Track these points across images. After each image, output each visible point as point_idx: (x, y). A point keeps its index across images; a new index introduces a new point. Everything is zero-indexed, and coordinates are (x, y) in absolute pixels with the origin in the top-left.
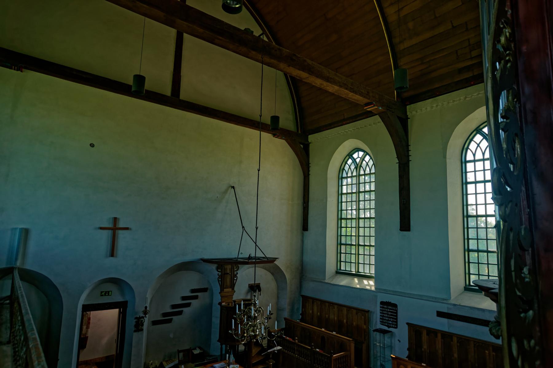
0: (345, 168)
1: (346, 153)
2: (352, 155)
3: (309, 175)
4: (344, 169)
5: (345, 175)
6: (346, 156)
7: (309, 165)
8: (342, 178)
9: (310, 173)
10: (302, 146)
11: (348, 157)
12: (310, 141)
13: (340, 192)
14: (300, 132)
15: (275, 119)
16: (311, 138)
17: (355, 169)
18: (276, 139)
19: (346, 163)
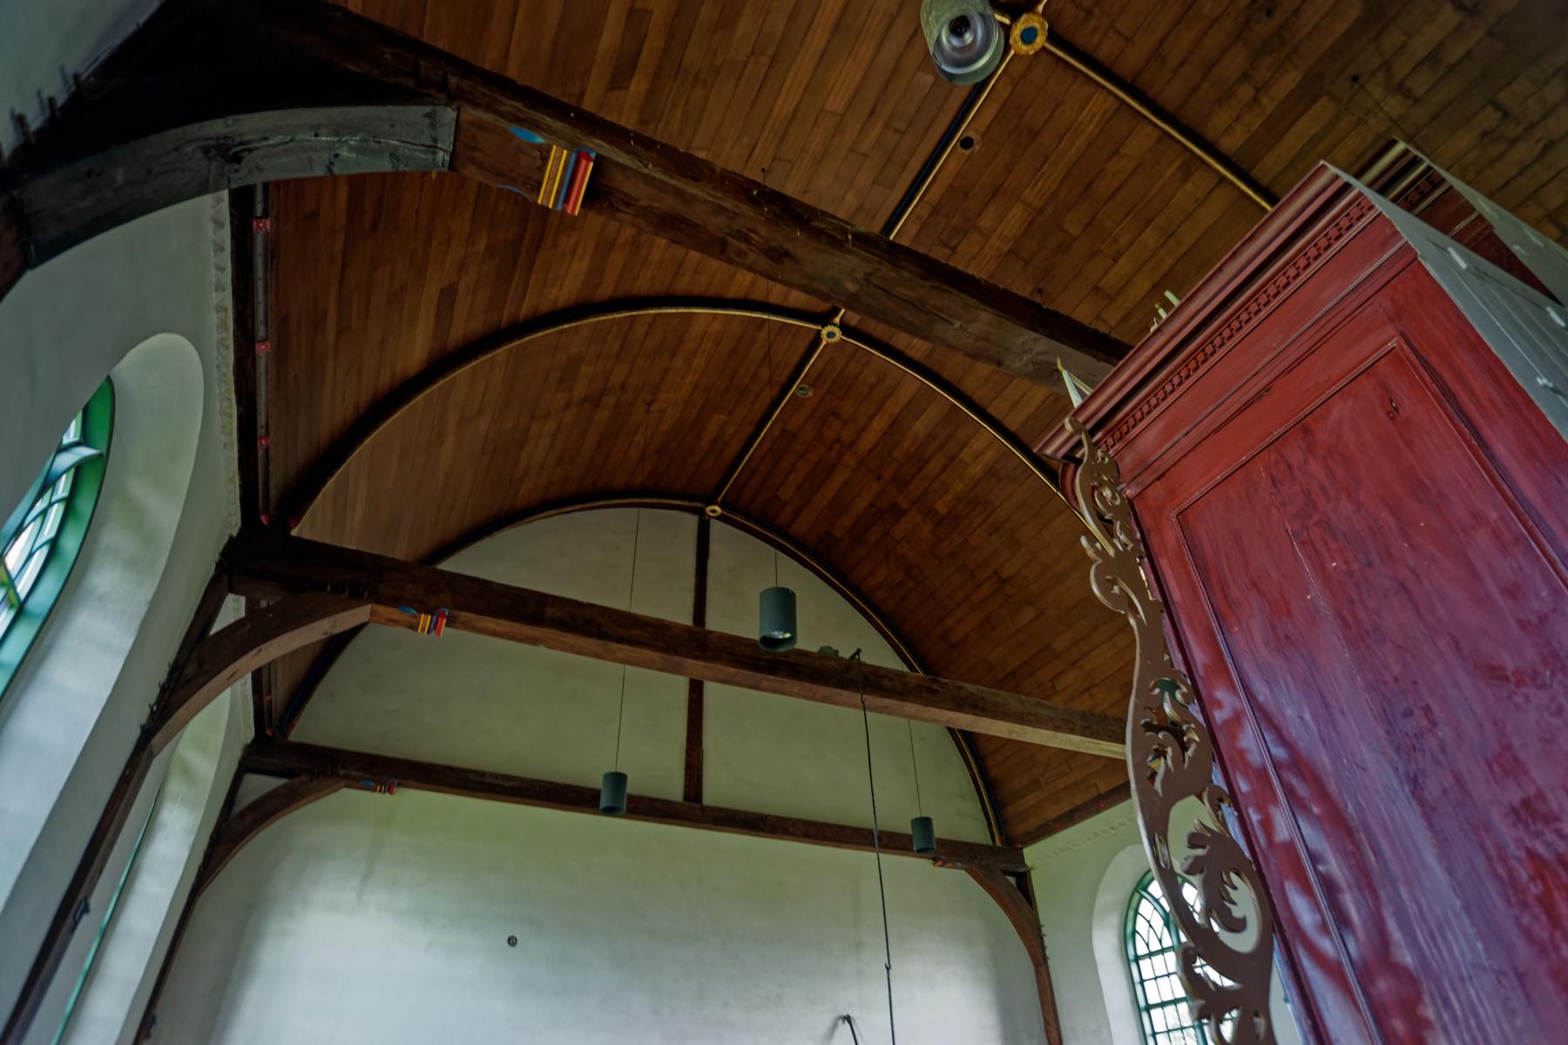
0: (1138, 928)
1: (1129, 884)
2: (1145, 889)
3: (1045, 958)
4: (1135, 932)
5: (1142, 950)
6: (1130, 893)
7: (1040, 931)
8: (1137, 959)
9: (1048, 952)
10: (1012, 880)
11: (1137, 896)
12: (1028, 861)
13: (1142, 1003)
14: (998, 843)
15: (924, 824)
16: (1031, 854)
17: (1165, 930)
18: (943, 870)
19: (1137, 913)
